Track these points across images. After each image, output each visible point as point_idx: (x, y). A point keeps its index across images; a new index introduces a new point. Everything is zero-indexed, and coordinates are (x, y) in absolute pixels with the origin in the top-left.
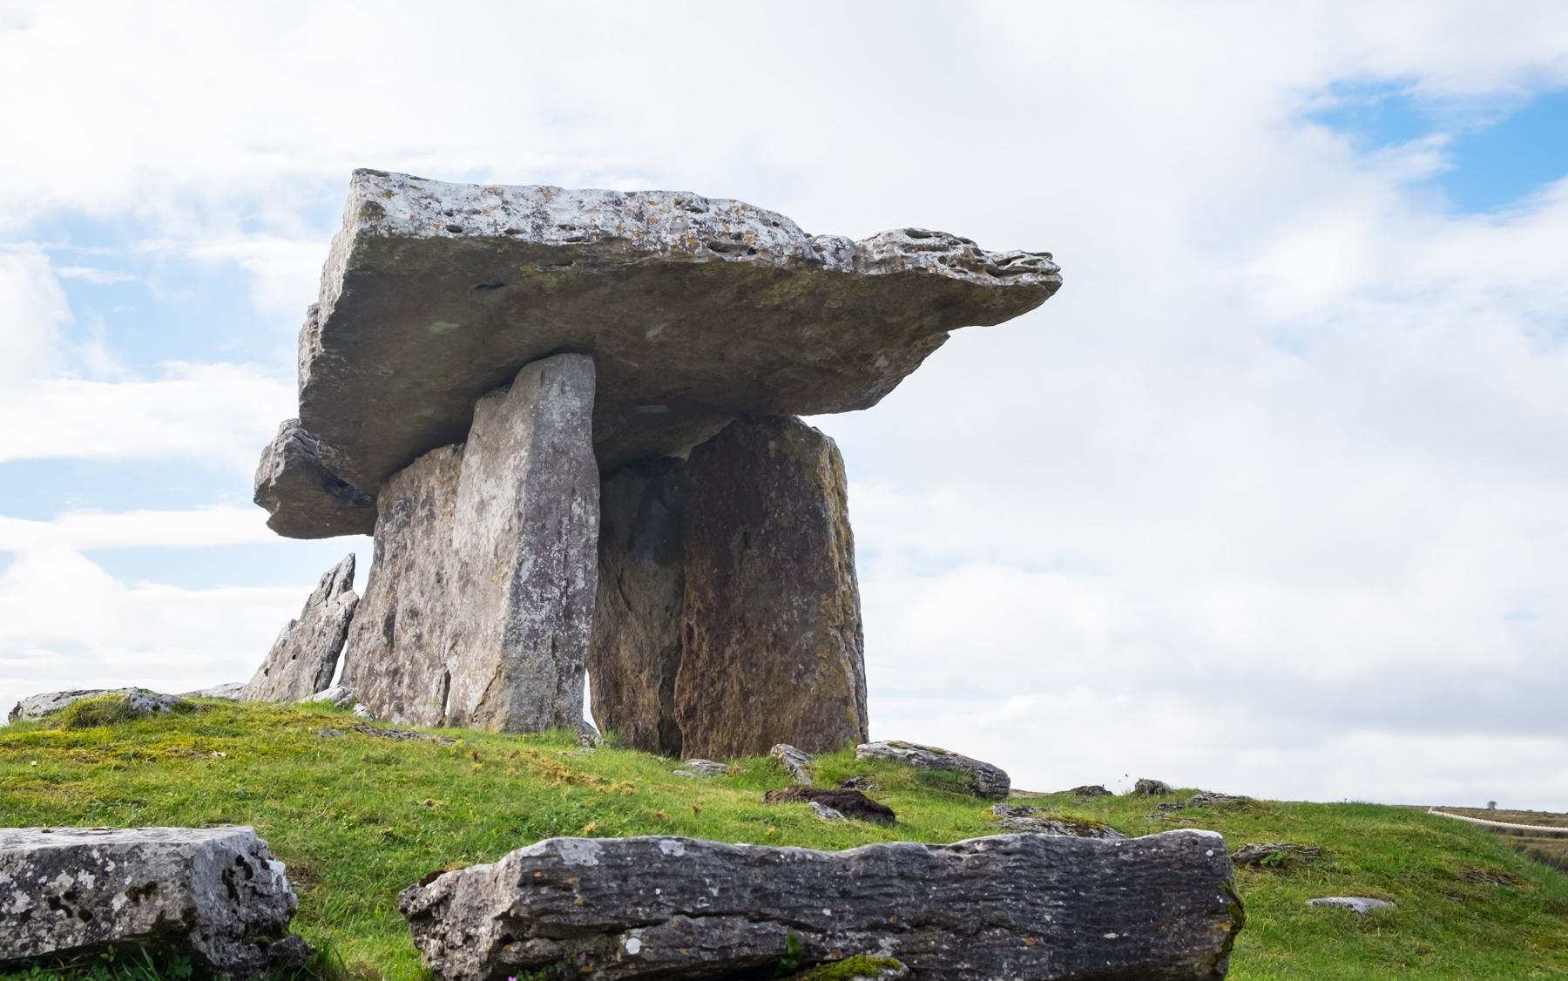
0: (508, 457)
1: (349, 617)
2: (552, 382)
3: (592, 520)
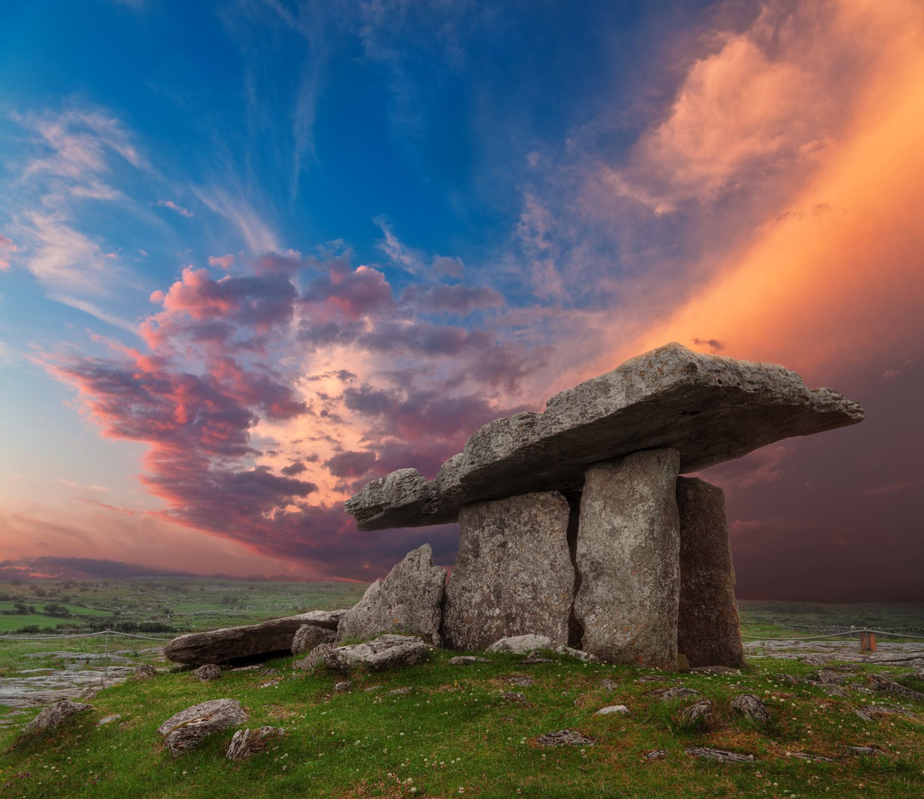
0: (634, 505)
1: (444, 581)
2: (664, 463)
3: (678, 540)
